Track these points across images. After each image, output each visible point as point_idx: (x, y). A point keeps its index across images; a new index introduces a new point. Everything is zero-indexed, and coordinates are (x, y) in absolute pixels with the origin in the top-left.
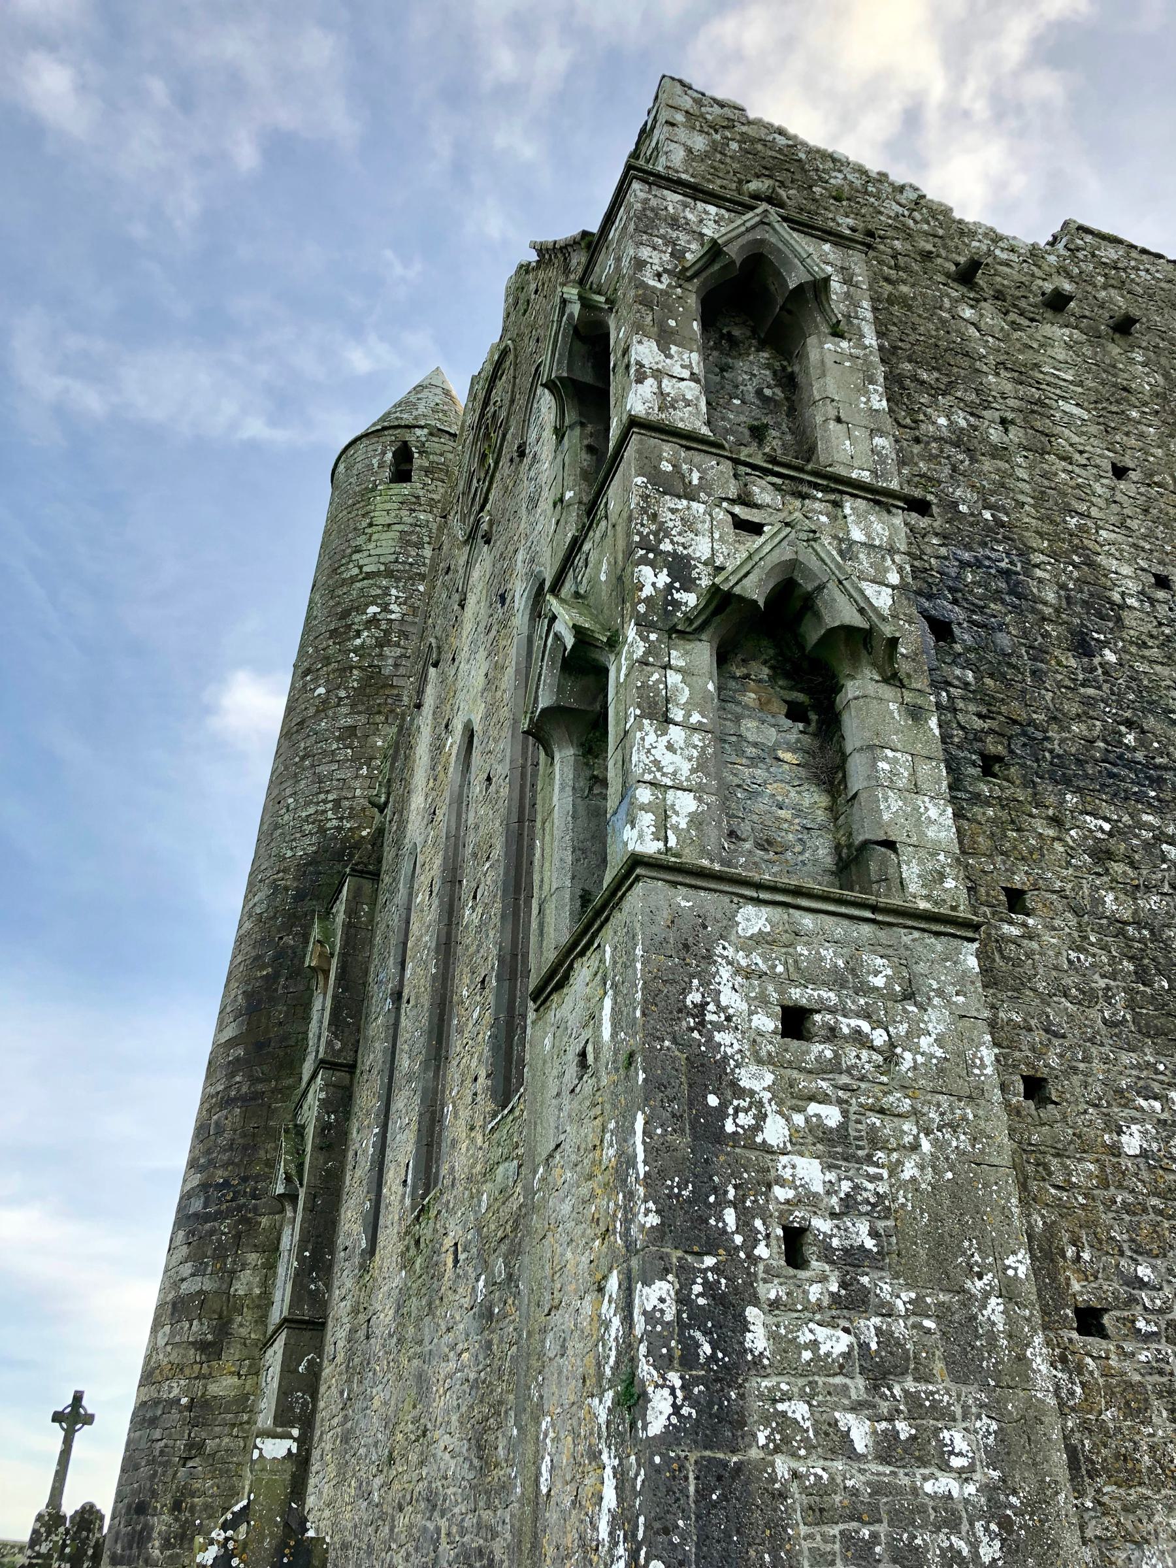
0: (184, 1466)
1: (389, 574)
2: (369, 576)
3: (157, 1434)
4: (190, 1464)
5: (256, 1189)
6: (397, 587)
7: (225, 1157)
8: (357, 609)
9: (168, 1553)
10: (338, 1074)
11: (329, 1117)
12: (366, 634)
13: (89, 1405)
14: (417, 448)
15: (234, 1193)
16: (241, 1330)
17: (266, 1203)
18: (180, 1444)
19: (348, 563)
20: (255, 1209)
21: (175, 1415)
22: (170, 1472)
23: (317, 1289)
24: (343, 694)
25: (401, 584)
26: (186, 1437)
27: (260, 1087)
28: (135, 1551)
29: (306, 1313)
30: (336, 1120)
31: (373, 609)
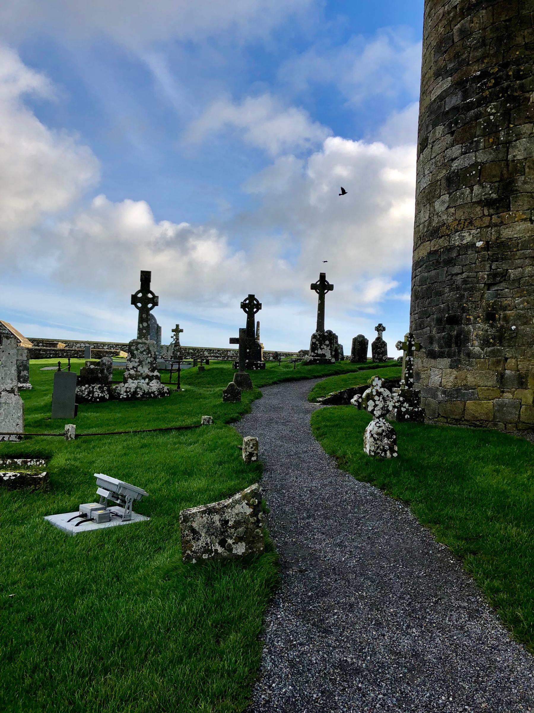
0: (488, 290)
3: (456, 269)
5: (520, 70)
9: (489, 349)
13: (329, 279)
15: (495, 79)
16: (526, 186)
18: (484, 275)
20: (522, 87)
21: (471, 255)
22: (477, 294)
26: (488, 269)
28: (454, 348)
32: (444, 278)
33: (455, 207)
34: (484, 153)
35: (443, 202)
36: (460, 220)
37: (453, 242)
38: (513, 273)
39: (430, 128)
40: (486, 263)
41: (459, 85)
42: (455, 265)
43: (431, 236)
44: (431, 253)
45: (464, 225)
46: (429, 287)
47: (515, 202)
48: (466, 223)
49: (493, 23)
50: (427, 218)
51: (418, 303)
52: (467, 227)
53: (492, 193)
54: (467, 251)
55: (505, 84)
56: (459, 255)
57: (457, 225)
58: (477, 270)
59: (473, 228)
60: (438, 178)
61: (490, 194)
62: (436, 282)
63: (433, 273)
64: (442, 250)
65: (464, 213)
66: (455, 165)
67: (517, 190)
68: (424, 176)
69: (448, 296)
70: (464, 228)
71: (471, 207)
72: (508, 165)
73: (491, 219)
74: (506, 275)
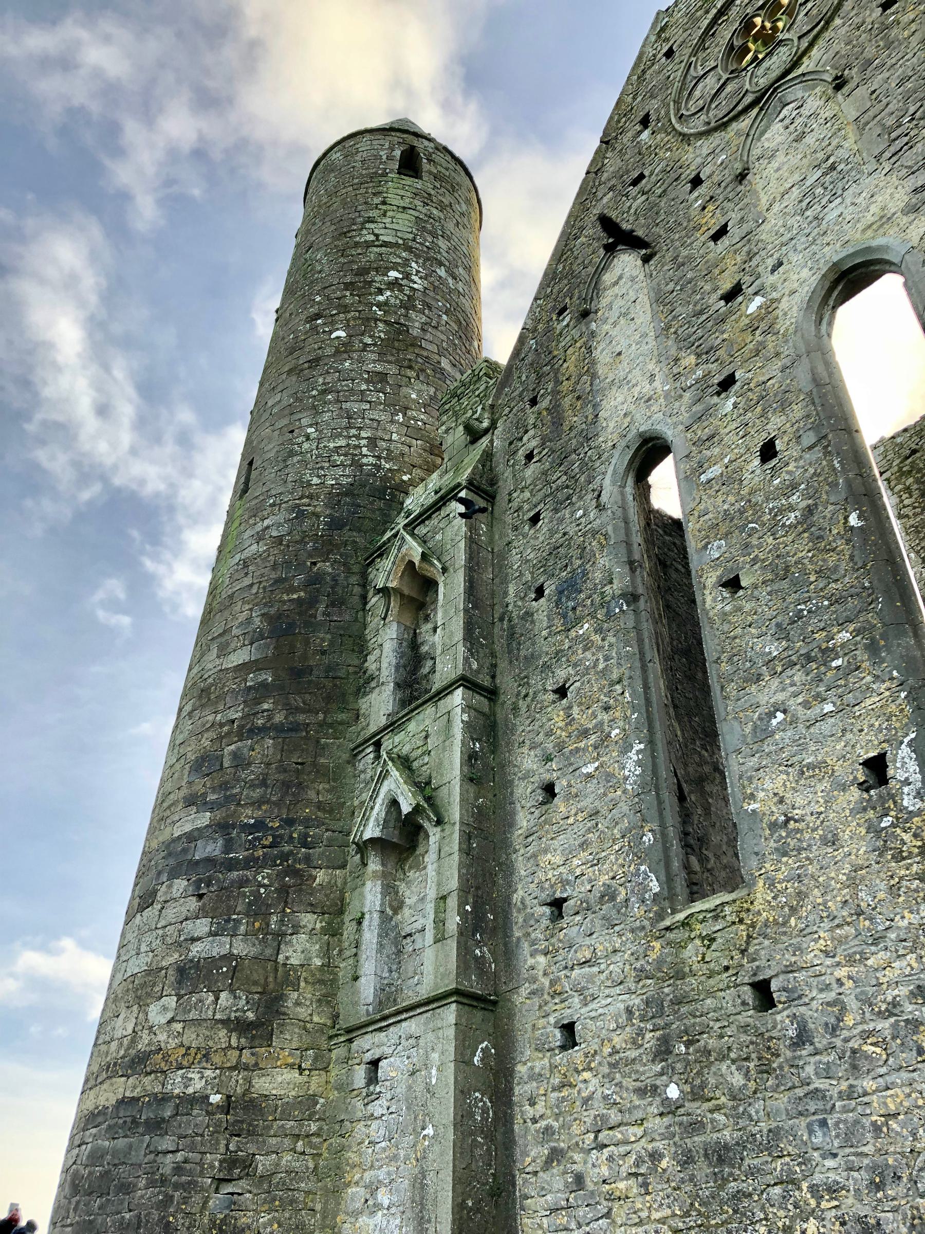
1: (409, 249)
2: (385, 244)
3: (167, 1143)
4: (229, 1188)
5: (306, 835)
6: (417, 262)
7: (257, 793)
8: (377, 270)
10: (478, 697)
11: (474, 744)
12: (388, 293)
14: (425, 155)
15: (274, 837)
16: (298, 1009)
17: (323, 853)
18: (214, 1159)
19: (361, 229)
20: (307, 859)
21: (199, 1116)
22: (197, 1199)
23: (483, 957)
24: (369, 341)
25: (421, 261)
26: (222, 1150)
27: (301, 718)
29: (474, 985)
30: (481, 749)
31: (393, 274)
32: (141, 1157)
33: (184, 1021)
34: (245, 941)
35: (165, 1009)
36: (189, 1048)
37: (169, 1087)
38: (263, 1163)
39: (164, 877)
40: (221, 1137)
41: (223, 827)
42: (166, 1133)
43: (131, 1067)
44: (122, 1102)
45: (195, 1059)
46: (107, 1172)
47: (281, 1032)
48: (199, 1056)
49: (281, 761)
50: (130, 1031)
51: (78, 1203)
52: (199, 1062)
53: (248, 1010)
54: (192, 1109)
55: (287, 848)
56: (177, 1114)
57: (183, 1055)
58: (203, 1149)
59: (210, 1067)
60: (164, 964)
61: (245, 1012)
62: (124, 1163)
63: (121, 1143)
64: (147, 1099)
65: (198, 1035)
66: (196, 950)
67: (284, 1014)
68: (138, 954)
69: (142, 1197)
70: (193, 1063)
71: (212, 1028)
72: (276, 970)
73: (240, 1056)
74: (251, 1165)
